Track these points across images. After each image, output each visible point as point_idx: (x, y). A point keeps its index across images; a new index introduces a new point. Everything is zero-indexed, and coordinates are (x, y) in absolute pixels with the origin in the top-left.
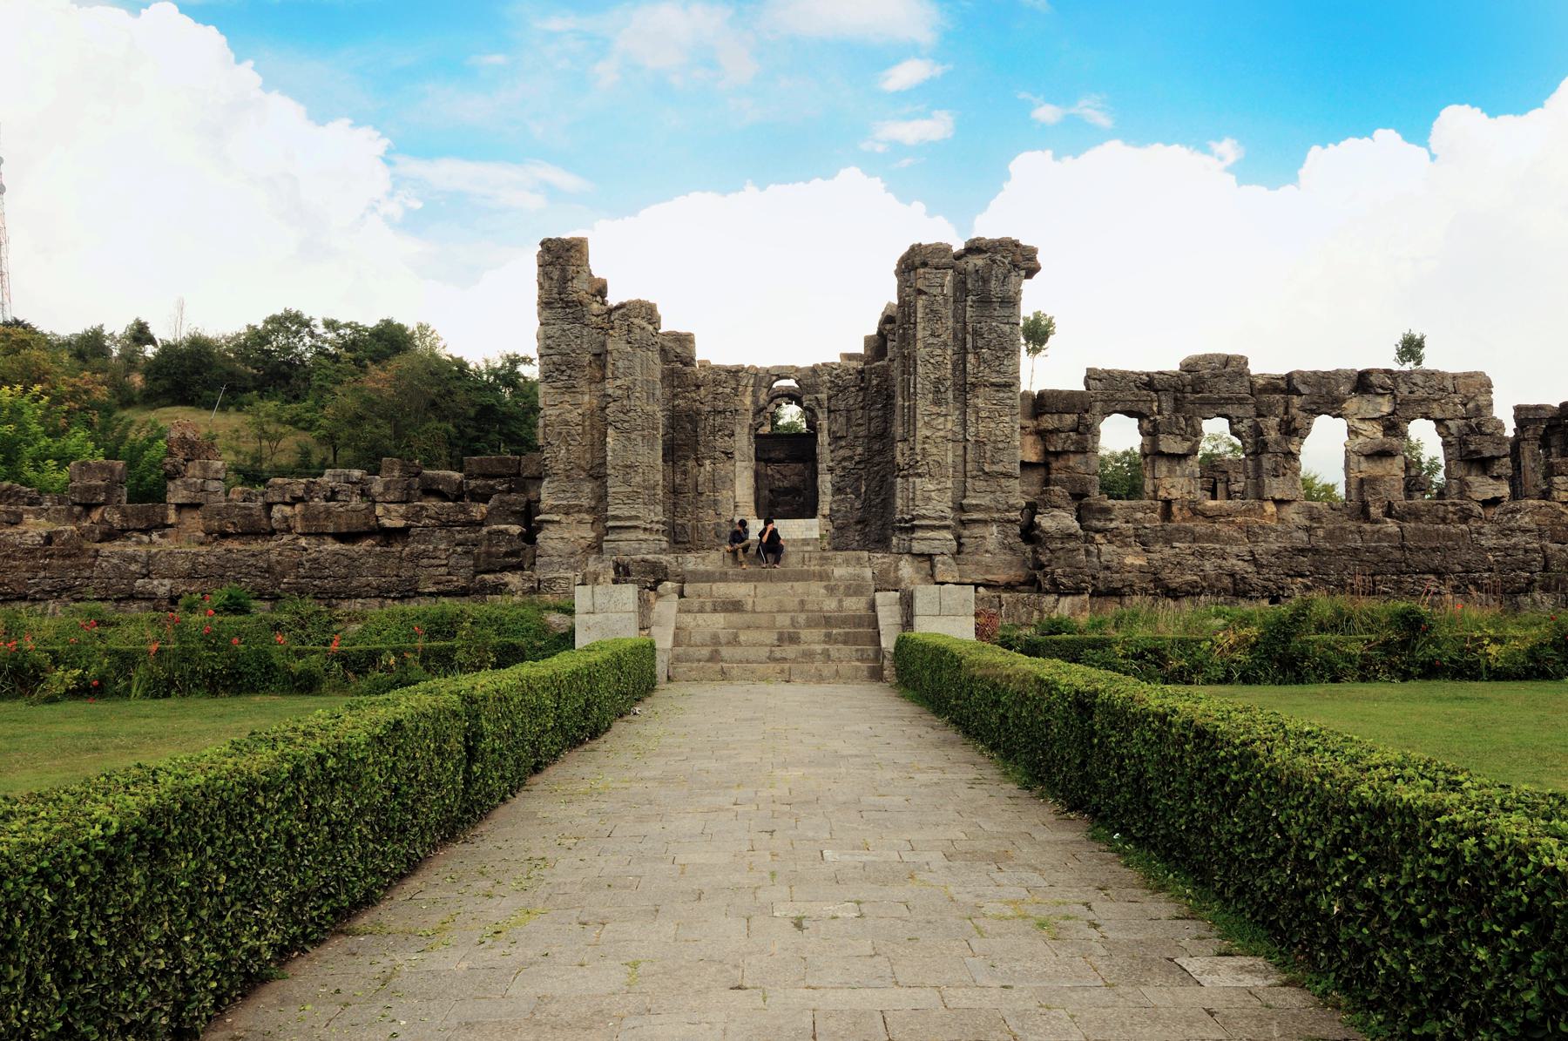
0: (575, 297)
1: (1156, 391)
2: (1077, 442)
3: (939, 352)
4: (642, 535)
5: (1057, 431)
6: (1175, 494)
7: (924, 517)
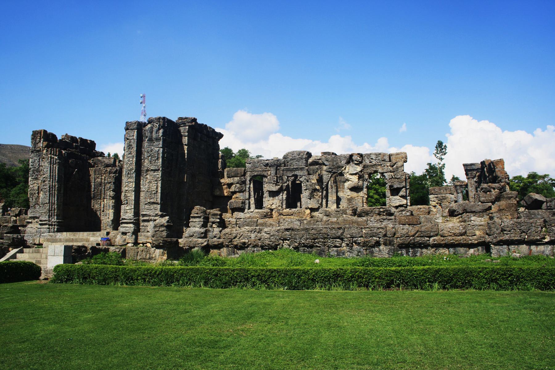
0: (38, 149)
1: (270, 167)
2: (238, 188)
3: (131, 159)
4: (47, 226)
5: (232, 184)
6: (274, 207)
7: (124, 219)
